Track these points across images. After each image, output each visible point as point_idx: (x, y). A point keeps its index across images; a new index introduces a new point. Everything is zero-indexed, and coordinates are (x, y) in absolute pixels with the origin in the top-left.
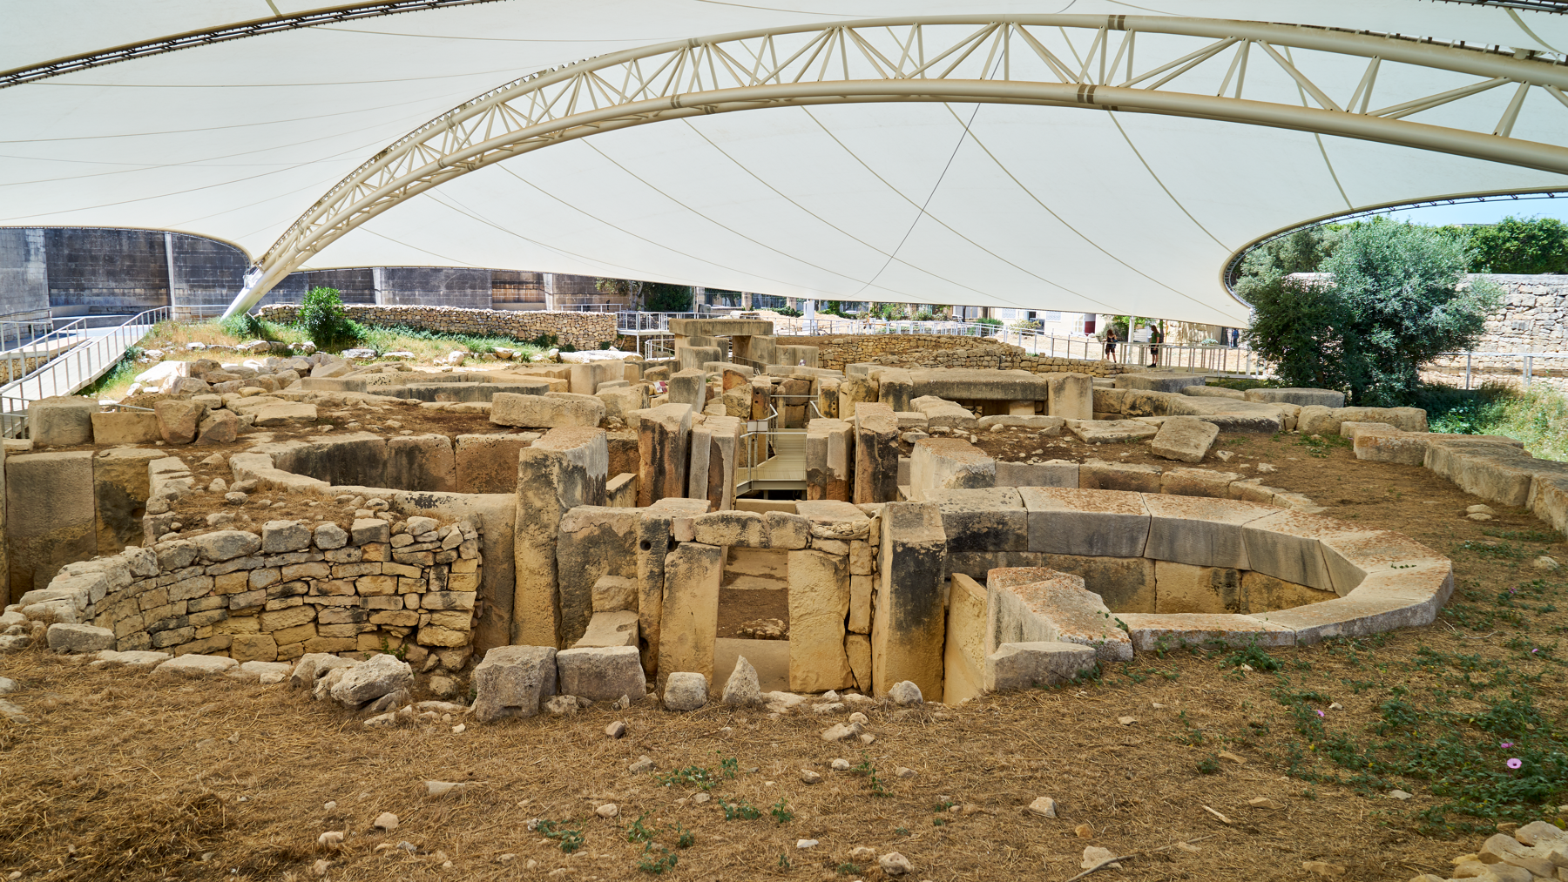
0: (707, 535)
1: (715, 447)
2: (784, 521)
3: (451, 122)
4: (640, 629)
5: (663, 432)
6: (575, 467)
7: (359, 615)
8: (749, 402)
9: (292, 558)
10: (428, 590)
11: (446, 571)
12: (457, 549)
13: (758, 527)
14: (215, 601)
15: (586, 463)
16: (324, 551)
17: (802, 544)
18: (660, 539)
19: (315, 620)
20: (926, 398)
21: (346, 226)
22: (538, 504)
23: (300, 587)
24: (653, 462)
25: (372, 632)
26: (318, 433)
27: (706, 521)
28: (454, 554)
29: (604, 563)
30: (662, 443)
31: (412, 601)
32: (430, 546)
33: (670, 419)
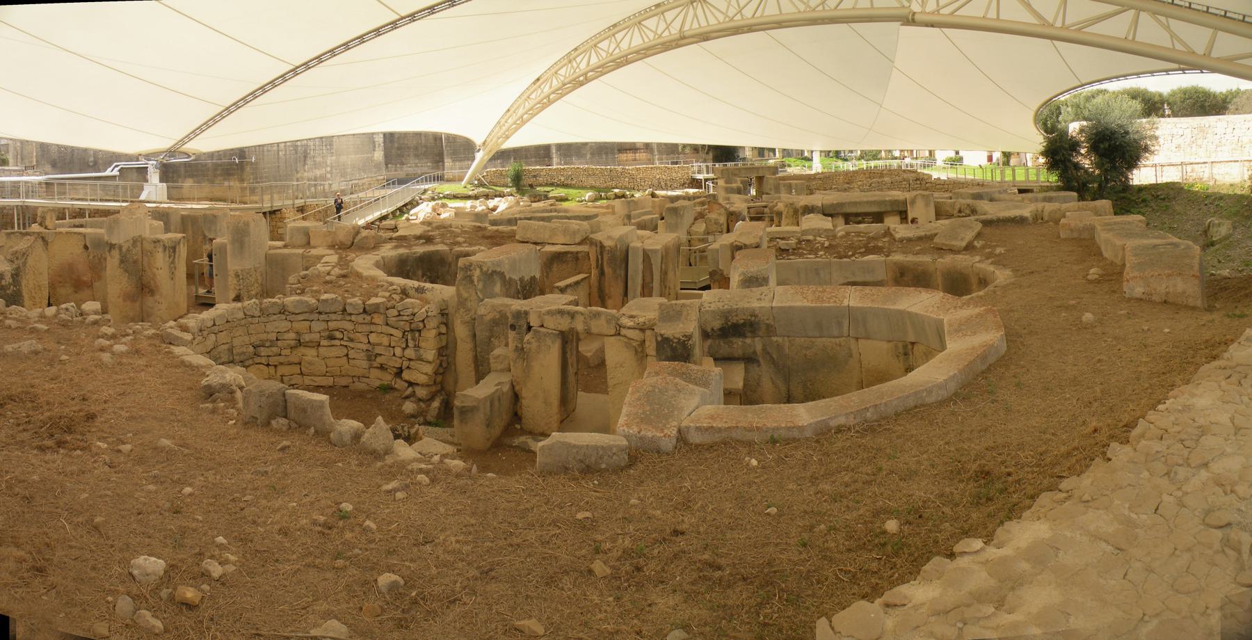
0: (551, 323)
1: (647, 256)
3: (569, 59)
5: (602, 247)
7: (371, 356)
13: (582, 318)
15: (505, 269)
17: (613, 332)
21: (522, 122)
22: (465, 295)
27: (550, 313)
28: (421, 325)
30: (601, 253)
31: (398, 351)
33: (610, 238)
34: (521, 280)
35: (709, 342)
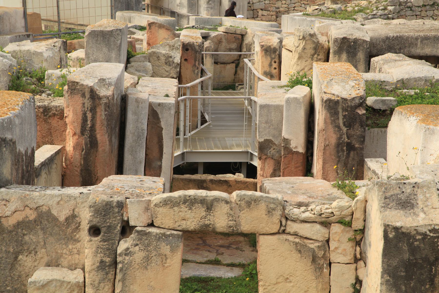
0: (168, 219)
1: (154, 114)
2: (256, 200)
8: (177, 60)
17: (276, 228)
18: (111, 225)
20: (389, 56)
24: (83, 132)
27: (166, 203)
29: (42, 252)
30: (93, 110)
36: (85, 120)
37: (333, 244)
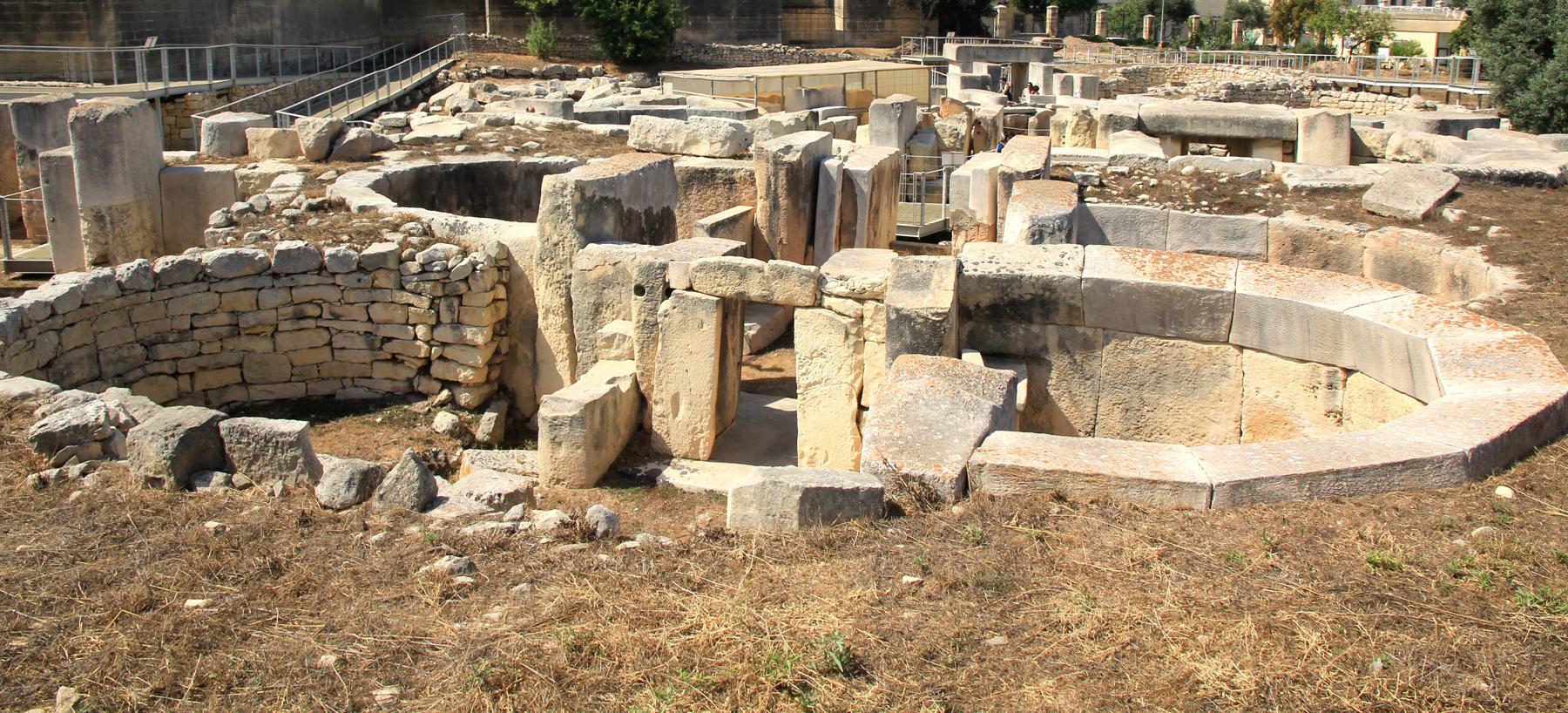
4: (636, 385)
6: (605, 199)
9: (302, 279)
10: (439, 323)
11: (456, 302)
12: (466, 279)
14: (223, 318)
16: (334, 274)
19: (330, 343)
23: (312, 310)
25: (386, 360)
26: (452, 152)
27: (703, 267)
30: (776, 174)
32: (438, 276)
34: (648, 212)
35: (969, 326)
36: (769, 184)
37: (866, 323)
